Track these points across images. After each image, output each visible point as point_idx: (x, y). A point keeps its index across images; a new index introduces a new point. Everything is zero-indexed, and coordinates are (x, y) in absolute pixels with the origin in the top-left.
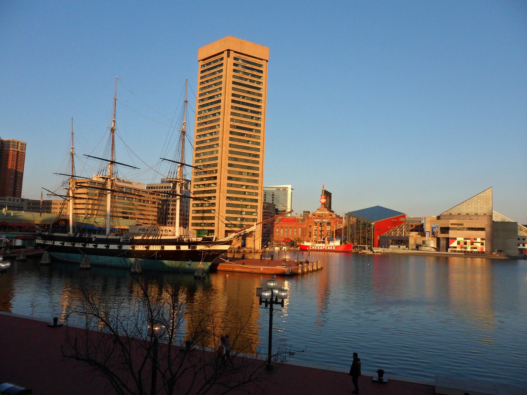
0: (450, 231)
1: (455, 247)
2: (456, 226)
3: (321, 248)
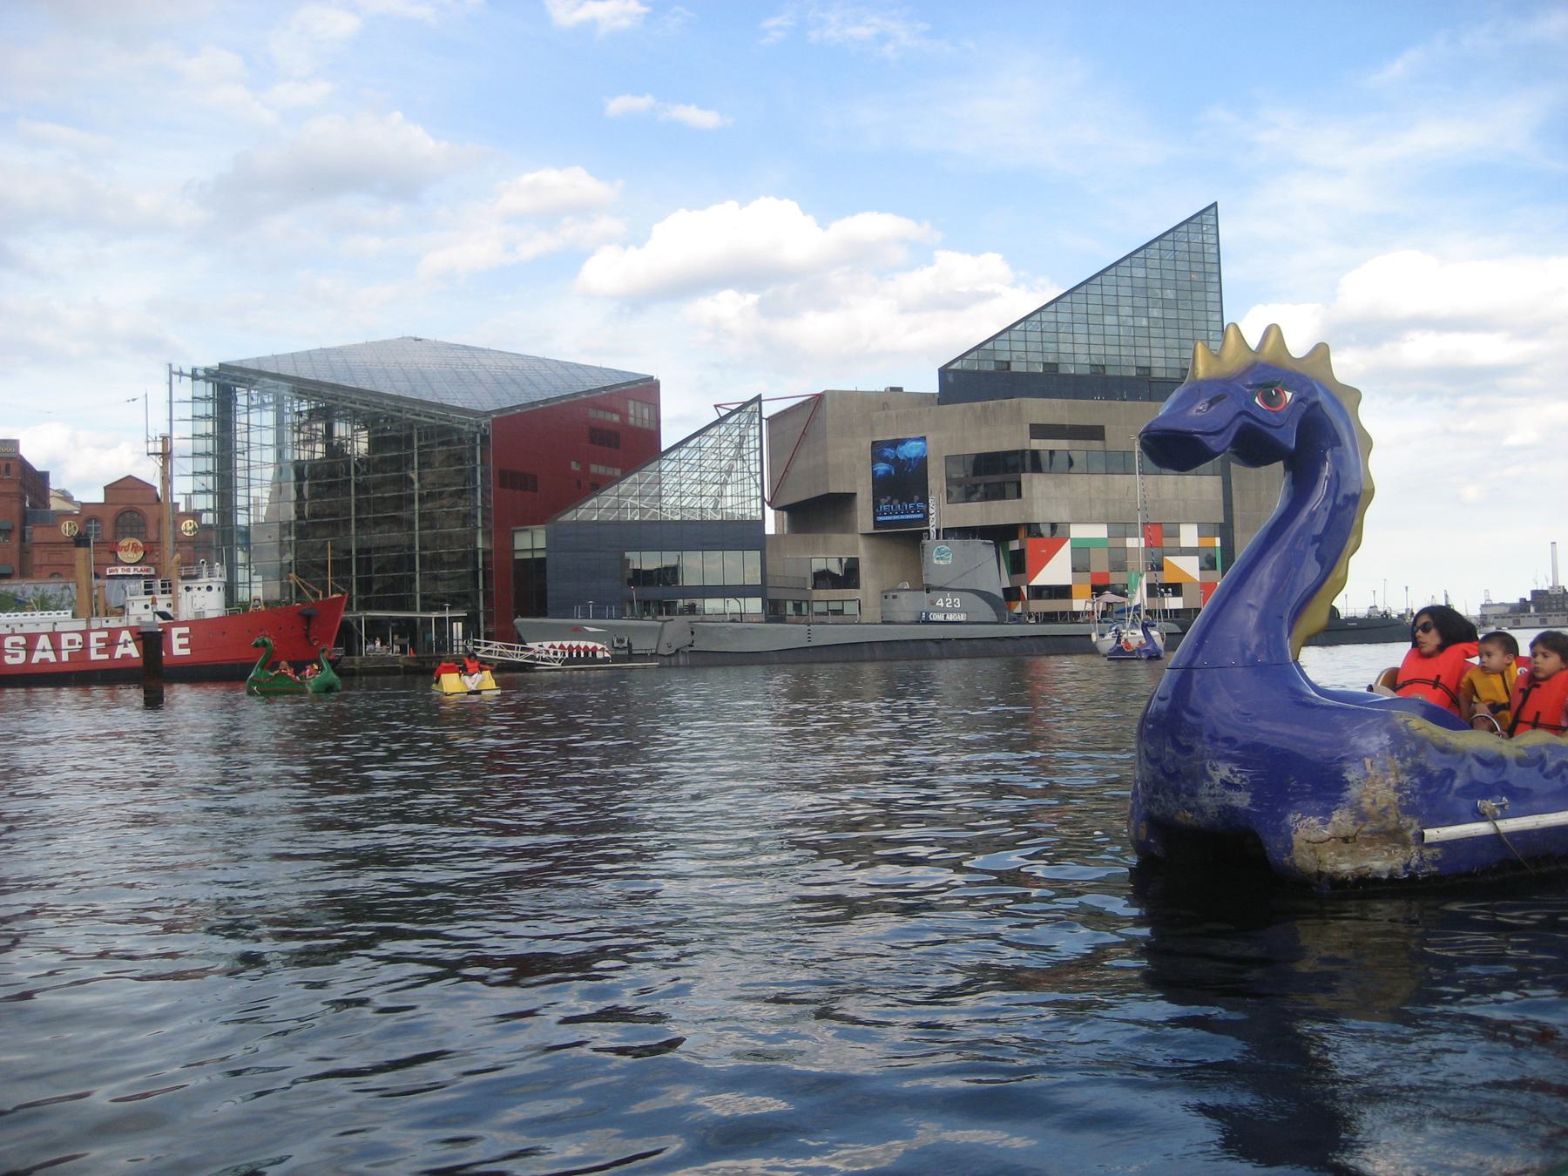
1: (1063, 592)
3: (43, 653)
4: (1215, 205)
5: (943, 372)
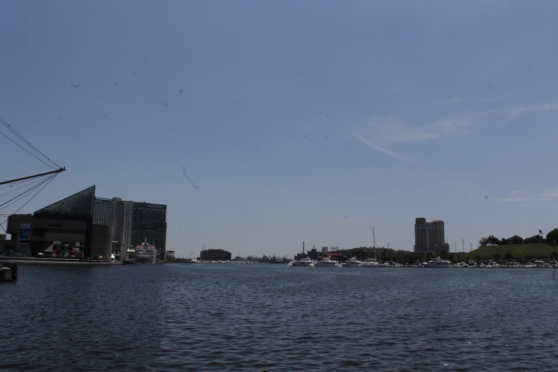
1: (51, 253)
2: (53, 227)
4: (95, 186)
5: (35, 213)
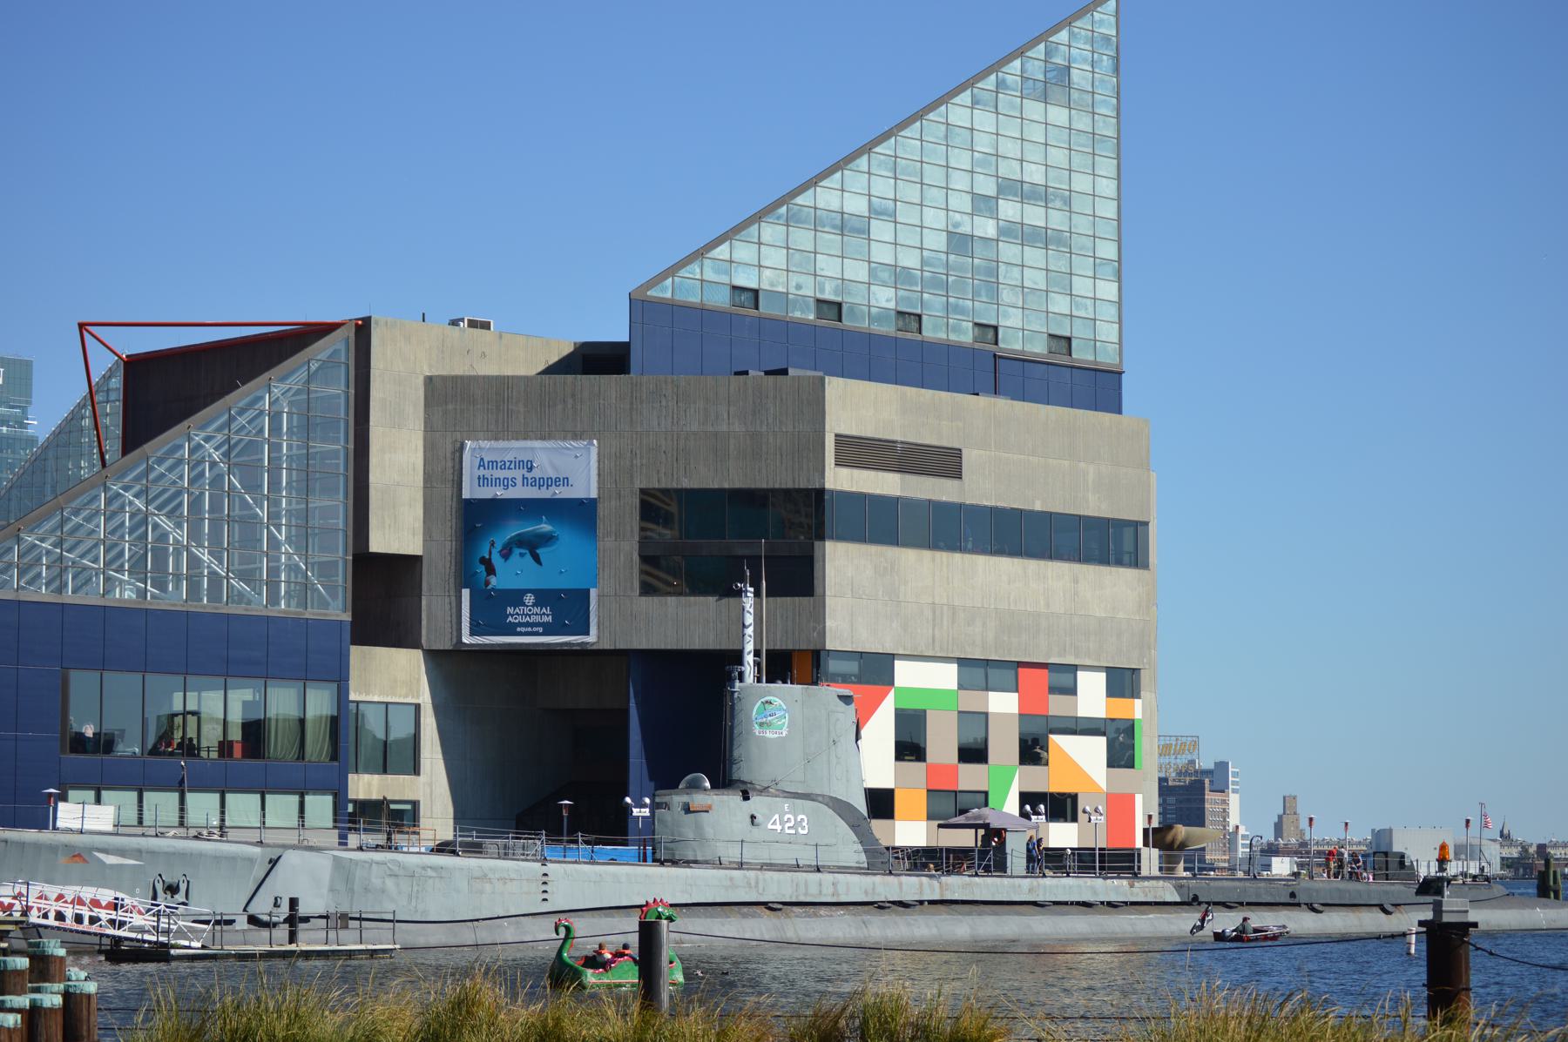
0: (844, 564)
2: (886, 484)
5: (641, 308)
